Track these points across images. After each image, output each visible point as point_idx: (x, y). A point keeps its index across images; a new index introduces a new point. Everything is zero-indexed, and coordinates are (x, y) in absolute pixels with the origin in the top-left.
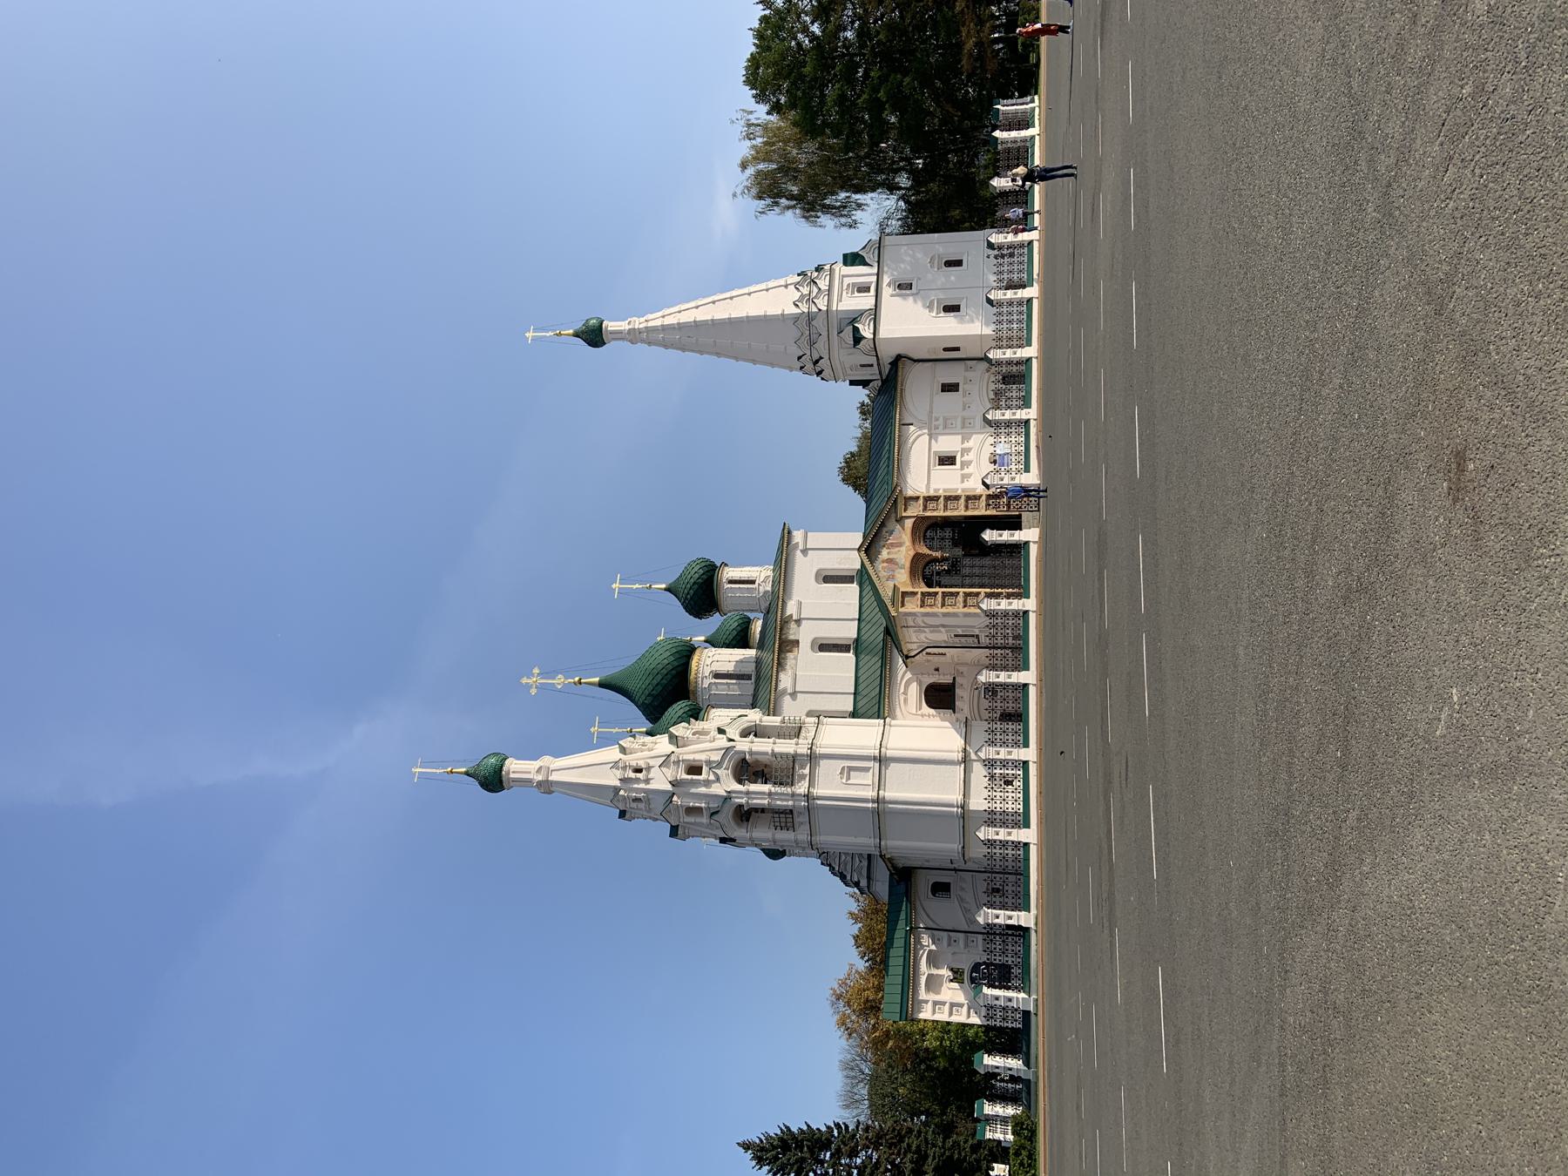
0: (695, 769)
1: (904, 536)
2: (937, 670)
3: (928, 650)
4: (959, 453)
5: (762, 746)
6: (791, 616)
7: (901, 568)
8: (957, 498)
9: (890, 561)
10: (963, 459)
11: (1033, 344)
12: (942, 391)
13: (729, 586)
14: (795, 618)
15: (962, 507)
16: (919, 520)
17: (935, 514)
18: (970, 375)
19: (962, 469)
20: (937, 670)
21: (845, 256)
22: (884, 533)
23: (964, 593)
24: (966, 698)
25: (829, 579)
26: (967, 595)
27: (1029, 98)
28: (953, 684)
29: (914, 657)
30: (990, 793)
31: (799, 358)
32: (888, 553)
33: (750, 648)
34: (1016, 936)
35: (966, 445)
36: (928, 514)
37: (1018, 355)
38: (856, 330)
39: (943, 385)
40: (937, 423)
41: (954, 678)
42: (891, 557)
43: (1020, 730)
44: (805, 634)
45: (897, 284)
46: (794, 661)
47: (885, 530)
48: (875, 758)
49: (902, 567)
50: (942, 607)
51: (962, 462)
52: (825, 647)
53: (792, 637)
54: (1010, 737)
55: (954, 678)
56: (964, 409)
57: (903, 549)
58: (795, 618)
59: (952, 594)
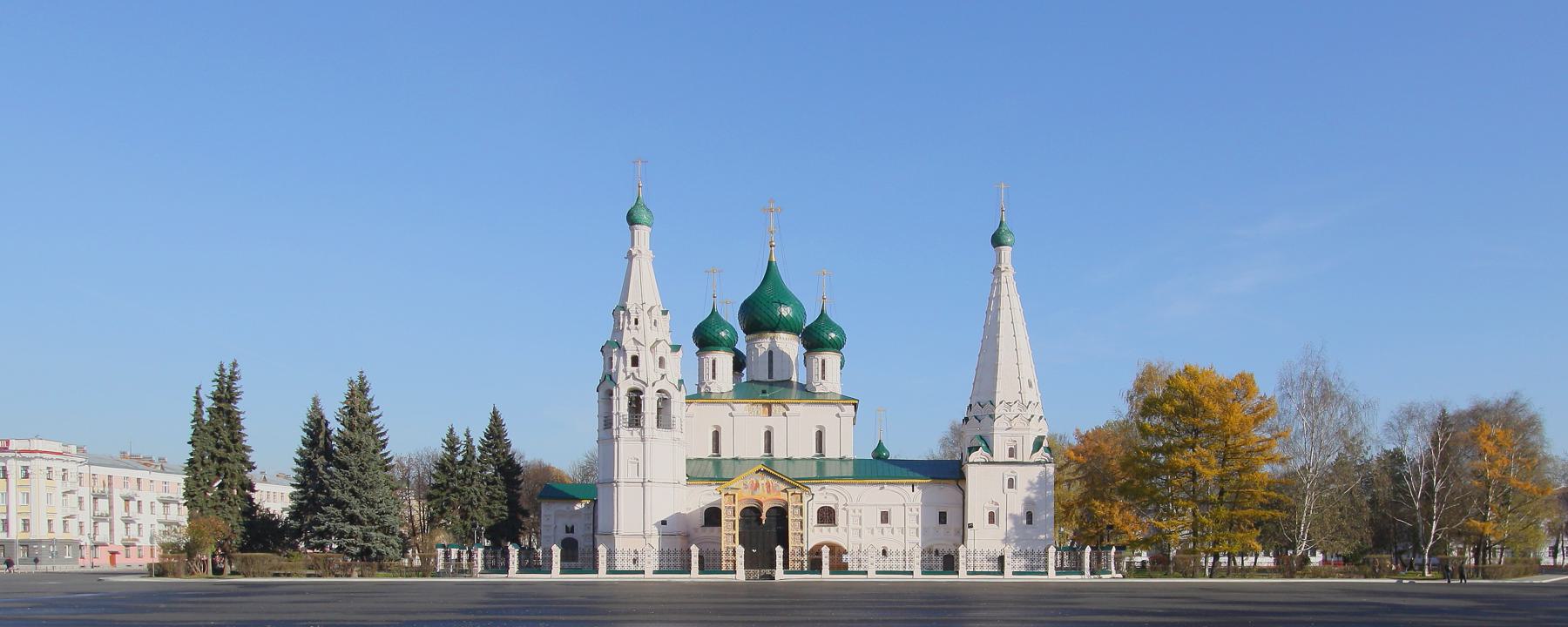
0: (635, 362)
6: (788, 410)
9: (757, 485)
13: (820, 361)
17: (790, 514)
18: (952, 532)
24: (712, 534)
35: (896, 531)
36: (790, 510)
38: (977, 449)
39: (945, 513)
44: (776, 421)
45: (1013, 478)
48: (644, 479)
49: (752, 493)
52: (768, 435)
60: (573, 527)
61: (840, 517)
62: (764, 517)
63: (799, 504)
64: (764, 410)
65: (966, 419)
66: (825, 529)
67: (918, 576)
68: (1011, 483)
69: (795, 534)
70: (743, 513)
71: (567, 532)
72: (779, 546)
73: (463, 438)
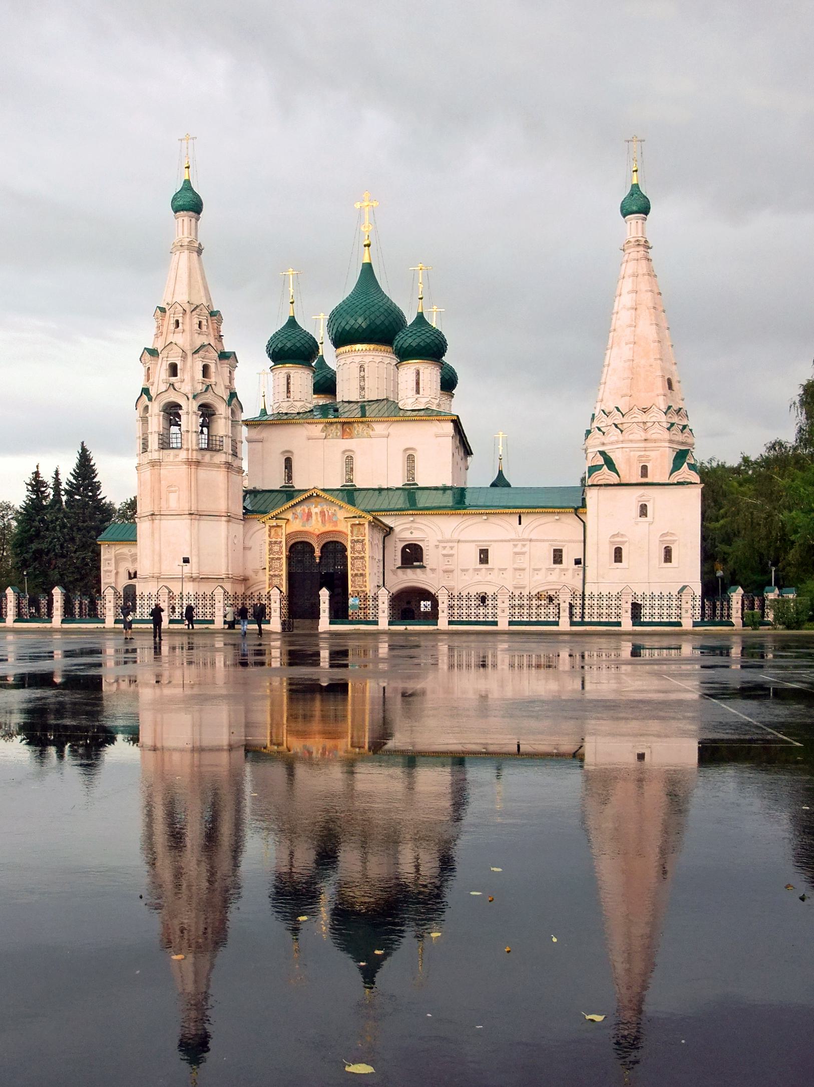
1: (332, 524)
5: (192, 423)
9: (309, 515)
10: (484, 570)
11: (331, 626)
12: (555, 550)
13: (415, 371)
14: (371, 433)
15: (356, 572)
17: (349, 550)
19: (476, 570)
22: (335, 508)
25: (411, 459)
26: (280, 576)
32: (316, 513)
38: (599, 467)
40: (520, 546)
47: (337, 508)
50: (270, 558)
51: (480, 570)
52: (349, 461)
53: (356, 432)
56: (535, 570)
58: (371, 433)
59: (281, 566)
60: (135, 573)
61: (430, 557)
62: (317, 553)
63: (360, 538)
64: (344, 431)
65: (588, 432)
66: (409, 571)
68: (643, 511)
69: (356, 575)
71: (130, 578)
72: (324, 589)
73: (51, 482)
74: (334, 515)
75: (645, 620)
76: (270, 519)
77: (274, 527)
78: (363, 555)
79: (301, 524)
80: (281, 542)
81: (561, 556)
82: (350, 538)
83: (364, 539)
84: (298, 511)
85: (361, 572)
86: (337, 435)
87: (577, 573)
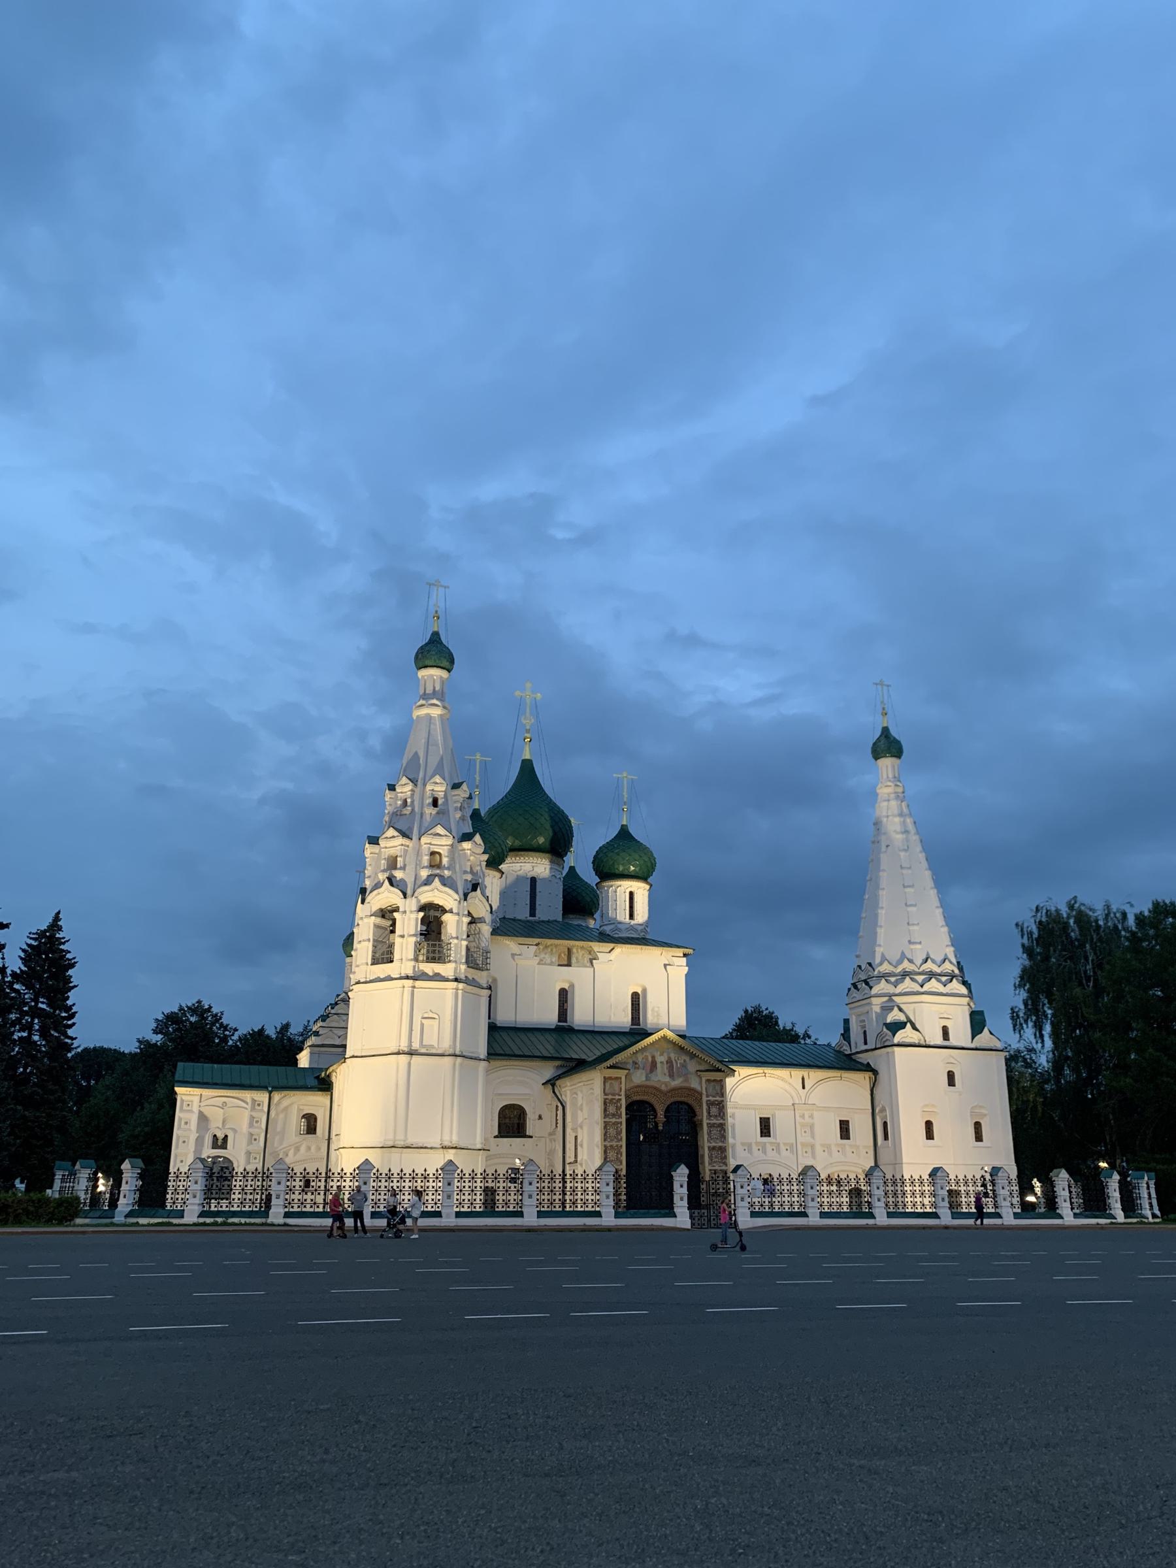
1: (681, 1080)
2: (540, 1117)
3: (560, 1107)
4: (774, 1141)
7: (646, 1077)
8: (723, 1137)
9: (654, 1065)
15: (714, 1144)
16: (701, 1094)
19: (757, 1143)
20: (540, 1117)
21: (981, 1013)
23: (621, 1146)
27: (1158, 1213)
28: (525, 1136)
29: (554, 1092)
30: (407, 1176)
31: (870, 964)
33: (563, 915)
34: (260, 1203)
35: (783, 1148)
36: (705, 1107)
37: (877, 1204)
41: (531, 1137)
42: (659, 1065)
43: (475, 1207)
46: (548, 961)
47: (687, 1059)
49: (647, 1079)
54: (467, 1197)
55: (531, 1137)
57: (667, 1079)
63: (718, 1098)
67: (609, 1219)
69: (714, 1148)
70: (629, 1107)
74: (684, 1066)
75: (988, 1211)
76: (608, 1068)
77: (610, 1078)
78: (721, 1121)
79: (644, 1079)
80: (620, 1099)
81: (847, 1130)
82: (704, 1099)
83: (723, 1101)
84: (640, 1059)
85: (720, 1144)
86: (552, 962)
87: (788, 1148)
